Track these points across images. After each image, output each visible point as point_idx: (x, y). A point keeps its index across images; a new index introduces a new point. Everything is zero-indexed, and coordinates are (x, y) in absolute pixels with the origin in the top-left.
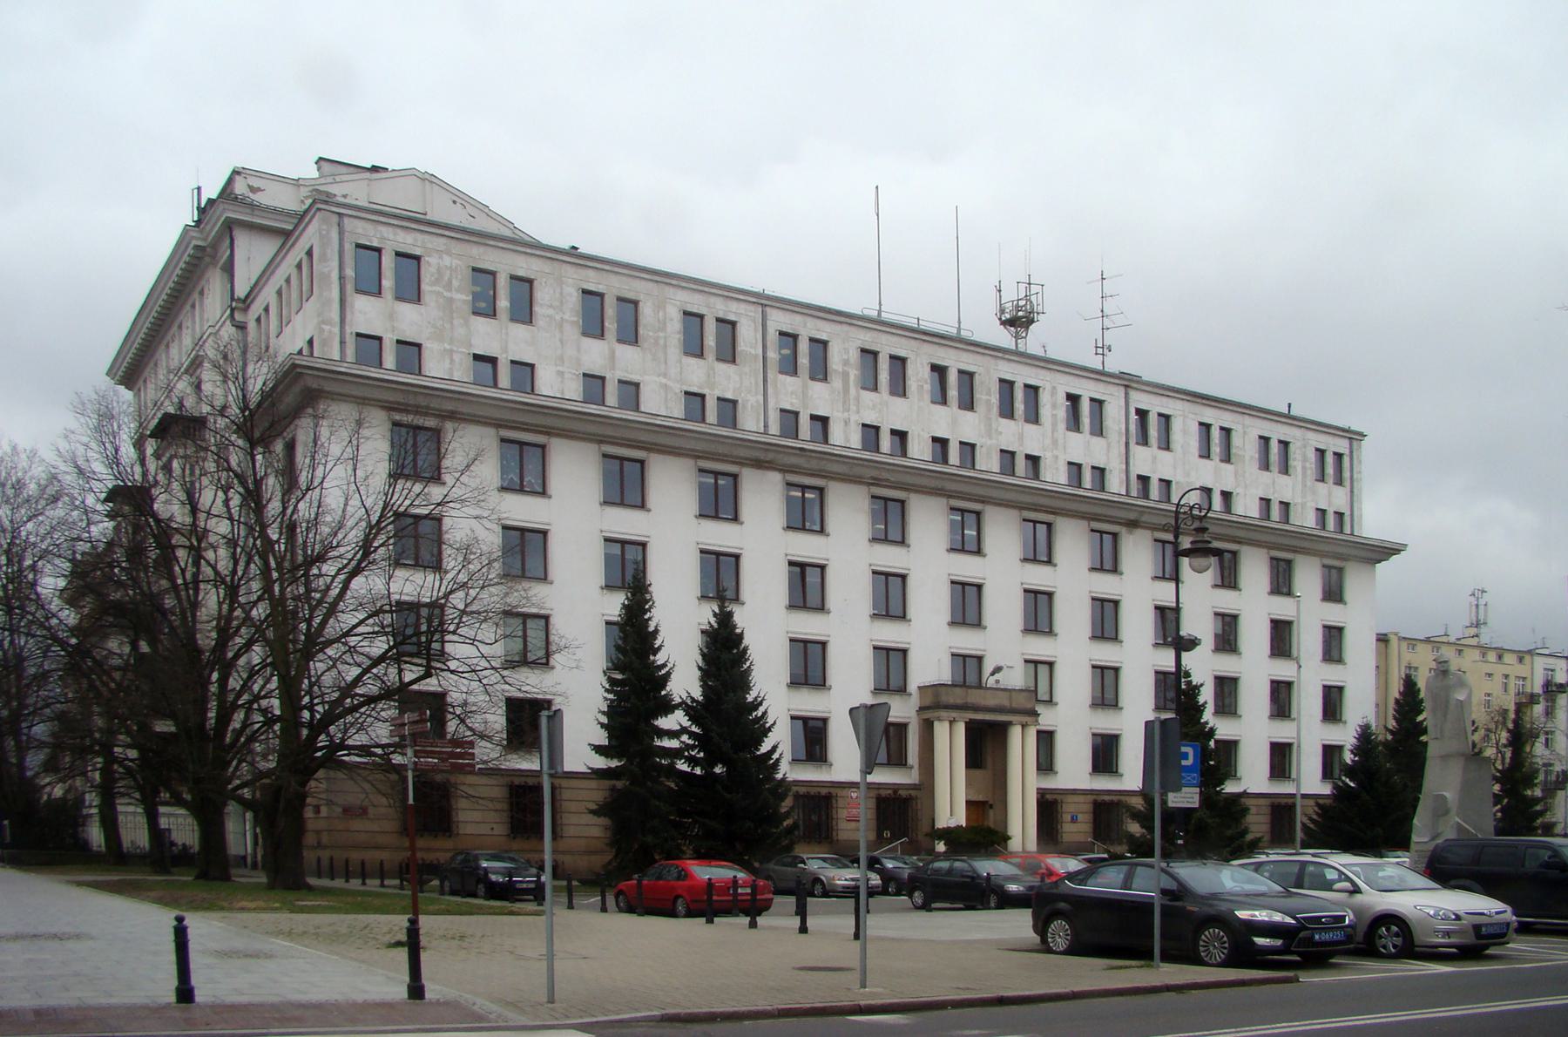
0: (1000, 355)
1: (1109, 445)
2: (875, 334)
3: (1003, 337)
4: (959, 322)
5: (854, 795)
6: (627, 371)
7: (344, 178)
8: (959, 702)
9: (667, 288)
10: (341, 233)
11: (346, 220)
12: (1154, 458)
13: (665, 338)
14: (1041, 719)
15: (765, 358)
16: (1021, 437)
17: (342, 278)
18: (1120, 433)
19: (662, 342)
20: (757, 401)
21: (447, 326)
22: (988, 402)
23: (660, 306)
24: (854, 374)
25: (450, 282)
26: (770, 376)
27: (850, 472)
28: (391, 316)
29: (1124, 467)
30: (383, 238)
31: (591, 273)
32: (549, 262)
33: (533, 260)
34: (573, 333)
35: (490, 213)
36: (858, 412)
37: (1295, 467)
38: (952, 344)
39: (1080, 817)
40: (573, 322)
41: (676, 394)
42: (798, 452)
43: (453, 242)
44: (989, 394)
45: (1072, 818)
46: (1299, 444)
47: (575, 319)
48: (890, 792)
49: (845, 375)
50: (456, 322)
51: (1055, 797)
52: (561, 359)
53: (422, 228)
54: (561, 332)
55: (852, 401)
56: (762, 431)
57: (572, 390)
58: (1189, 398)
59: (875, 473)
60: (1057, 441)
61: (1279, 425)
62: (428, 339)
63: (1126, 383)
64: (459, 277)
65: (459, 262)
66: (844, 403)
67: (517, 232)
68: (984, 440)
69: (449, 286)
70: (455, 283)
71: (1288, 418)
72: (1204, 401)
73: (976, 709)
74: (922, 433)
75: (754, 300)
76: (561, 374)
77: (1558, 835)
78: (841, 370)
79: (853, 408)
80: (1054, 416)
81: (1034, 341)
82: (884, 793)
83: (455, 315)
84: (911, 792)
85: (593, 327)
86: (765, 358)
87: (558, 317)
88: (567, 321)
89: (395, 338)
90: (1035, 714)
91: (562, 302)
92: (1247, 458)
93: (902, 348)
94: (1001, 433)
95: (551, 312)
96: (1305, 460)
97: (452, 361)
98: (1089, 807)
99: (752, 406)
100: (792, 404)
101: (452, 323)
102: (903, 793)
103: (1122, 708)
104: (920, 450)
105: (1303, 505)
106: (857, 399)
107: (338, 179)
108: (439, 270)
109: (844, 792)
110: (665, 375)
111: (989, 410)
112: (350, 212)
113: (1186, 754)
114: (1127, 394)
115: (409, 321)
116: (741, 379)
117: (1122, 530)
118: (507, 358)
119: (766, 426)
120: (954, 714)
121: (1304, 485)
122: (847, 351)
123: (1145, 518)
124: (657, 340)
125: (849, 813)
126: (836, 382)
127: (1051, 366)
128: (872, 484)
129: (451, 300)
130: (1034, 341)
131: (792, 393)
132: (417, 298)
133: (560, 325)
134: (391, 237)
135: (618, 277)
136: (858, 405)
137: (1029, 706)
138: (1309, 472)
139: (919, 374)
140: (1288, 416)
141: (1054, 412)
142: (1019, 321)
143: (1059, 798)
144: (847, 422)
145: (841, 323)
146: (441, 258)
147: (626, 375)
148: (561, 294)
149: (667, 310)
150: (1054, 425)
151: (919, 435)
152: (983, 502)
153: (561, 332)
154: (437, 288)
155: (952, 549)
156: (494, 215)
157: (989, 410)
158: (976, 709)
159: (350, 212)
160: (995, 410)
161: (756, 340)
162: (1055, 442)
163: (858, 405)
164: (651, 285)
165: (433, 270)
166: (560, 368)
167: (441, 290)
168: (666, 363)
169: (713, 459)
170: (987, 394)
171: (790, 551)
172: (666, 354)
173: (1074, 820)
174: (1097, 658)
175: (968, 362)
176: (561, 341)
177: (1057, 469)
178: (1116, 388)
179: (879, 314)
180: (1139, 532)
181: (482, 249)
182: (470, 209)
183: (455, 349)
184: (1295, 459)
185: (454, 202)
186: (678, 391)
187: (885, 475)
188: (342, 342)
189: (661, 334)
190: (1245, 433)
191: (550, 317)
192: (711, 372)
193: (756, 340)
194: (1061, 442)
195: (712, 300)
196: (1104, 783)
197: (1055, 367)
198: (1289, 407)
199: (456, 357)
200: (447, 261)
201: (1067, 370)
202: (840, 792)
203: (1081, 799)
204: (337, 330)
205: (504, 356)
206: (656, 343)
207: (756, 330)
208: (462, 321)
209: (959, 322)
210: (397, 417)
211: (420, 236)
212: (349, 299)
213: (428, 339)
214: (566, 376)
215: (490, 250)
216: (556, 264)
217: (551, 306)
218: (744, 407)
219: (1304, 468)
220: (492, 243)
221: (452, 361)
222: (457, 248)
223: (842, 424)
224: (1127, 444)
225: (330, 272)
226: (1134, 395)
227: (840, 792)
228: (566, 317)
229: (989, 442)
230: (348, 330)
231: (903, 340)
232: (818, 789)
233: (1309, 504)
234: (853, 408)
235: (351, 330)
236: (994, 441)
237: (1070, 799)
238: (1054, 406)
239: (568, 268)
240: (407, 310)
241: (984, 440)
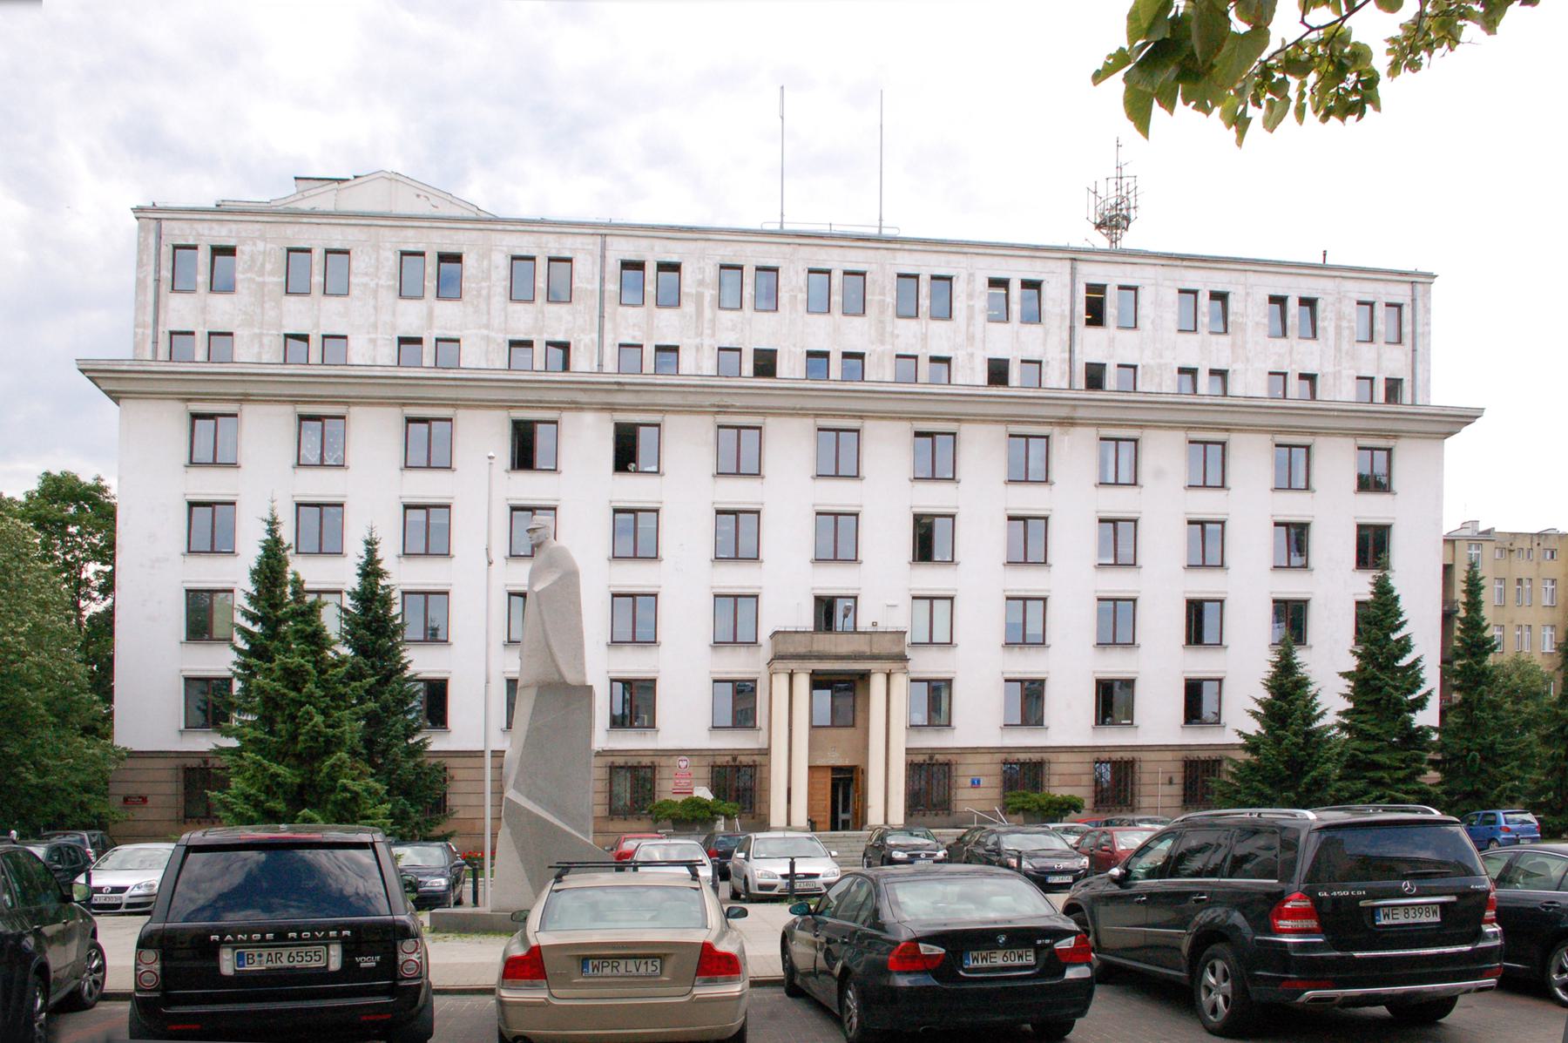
0: (898, 246)
1: (1046, 333)
2: (737, 246)
3: (1101, 241)
4: (881, 220)
5: (683, 764)
6: (446, 329)
7: (312, 192)
8: (802, 650)
9: (494, 235)
10: (159, 237)
11: (164, 224)
12: (542, 312)
13: (489, 287)
14: (910, 665)
15: (602, 292)
16: (925, 338)
17: (158, 281)
18: (1062, 316)
19: (484, 292)
20: (592, 340)
21: (258, 311)
22: (882, 303)
23: (485, 255)
24: (710, 294)
25: (263, 265)
26: (608, 310)
27: (887, 407)
28: (204, 309)
29: (1067, 355)
30: (199, 235)
31: (410, 233)
32: (366, 229)
33: (350, 230)
34: (388, 297)
35: (454, 201)
36: (713, 335)
37: (1325, 329)
38: (834, 243)
39: (968, 782)
40: (389, 286)
41: (499, 344)
42: (616, 387)
43: (268, 226)
44: (883, 293)
45: (973, 783)
46: (1330, 299)
47: (392, 283)
48: (729, 758)
49: (699, 297)
50: (267, 306)
51: (949, 757)
52: (375, 326)
53: (235, 218)
54: (376, 298)
55: (706, 325)
56: (596, 370)
57: (386, 354)
58: (1163, 262)
59: (716, 400)
60: (973, 337)
61: (1301, 279)
62: (238, 326)
63: (1073, 256)
64: (273, 260)
65: (274, 246)
66: (697, 327)
67: (479, 212)
68: (874, 347)
69: (261, 273)
70: (268, 267)
71: (1322, 269)
72: (1185, 263)
73: (821, 657)
74: (793, 349)
75: (591, 231)
76: (373, 341)
77: (777, 829)
78: (694, 291)
79: (707, 331)
80: (971, 308)
81: (1129, 240)
82: (720, 760)
83: (266, 298)
84: (756, 758)
85: (518, 293)
86: (602, 292)
87: (372, 284)
88: (382, 286)
89: (207, 331)
90: (902, 658)
91: (377, 268)
92: (1250, 324)
93: (856, 259)
94: (898, 336)
95: (365, 280)
96: (1340, 317)
97: (261, 345)
98: (997, 769)
99: (585, 346)
100: (634, 337)
101: (263, 307)
102: (745, 760)
103: (1226, 647)
104: (880, 371)
105: (1337, 375)
106: (713, 321)
107: (306, 194)
108: (253, 259)
109: (671, 761)
110: (487, 326)
111: (882, 312)
112: (165, 216)
113: (308, 713)
114: (1073, 269)
115: (222, 311)
116: (574, 318)
117: (1055, 432)
118: (317, 334)
119: (600, 365)
120: (793, 665)
121: (1338, 349)
122: (702, 270)
123: (1080, 413)
124: (479, 291)
125: (676, 784)
126: (688, 306)
127: (966, 250)
128: (718, 413)
129: (263, 284)
130: (1129, 240)
131: (634, 325)
132: (230, 289)
133: (375, 292)
134: (206, 232)
135: (440, 232)
136: (713, 328)
137: (896, 650)
138: (1346, 333)
139: (793, 281)
140: (1323, 267)
141: (971, 303)
142: (1113, 222)
143: (952, 758)
144: (699, 348)
145: (696, 240)
146: (255, 244)
147: (446, 332)
148: (377, 259)
149: (493, 257)
150: (970, 318)
151: (790, 351)
152: (861, 417)
153: (376, 298)
154: (249, 275)
155: (818, 476)
156: (458, 202)
157: (882, 312)
158: (821, 657)
159: (165, 216)
160: (891, 311)
161: (593, 274)
162: (971, 338)
163: (713, 328)
164: (474, 233)
165: (246, 257)
166: (373, 336)
167: (253, 276)
168: (489, 314)
169: (834, 416)
170: (880, 294)
171: (717, 499)
172: (488, 305)
173: (975, 784)
174: (1012, 587)
175: (856, 259)
176: (375, 308)
177: (972, 369)
178: (1059, 263)
179: (782, 227)
180: (1079, 430)
181: (297, 228)
182: (434, 200)
183: (265, 332)
184: (1324, 319)
185: (418, 196)
186: (500, 341)
187: (728, 401)
188: (155, 342)
189: (484, 284)
190: (1247, 294)
191: (365, 285)
192: (540, 316)
193: (593, 274)
194: (979, 336)
195: (545, 238)
196: (1113, 737)
197: (972, 250)
198: (1325, 255)
199: (266, 340)
200: (261, 246)
201: (947, 249)
202: (663, 761)
203: (986, 758)
204: (150, 332)
205: (315, 331)
206: (479, 295)
207: (594, 263)
208: (273, 304)
209: (881, 220)
210: (724, 419)
211: (234, 226)
212: (162, 298)
213: (238, 326)
214: (380, 342)
215: (305, 227)
216: (372, 230)
217: (366, 274)
218: (576, 348)
219: (1338, 329)
220: (305, 220)
221: (261, 345)
222: (271, 231)
223: (694, 350)
224: (1072, 328)
225: (145, 277)
226: (1081, 267)
227: (663, 761)
228: (382, 282)
229: (880, 348)
230: (161, 329)
231: (774, 247)
232: (640, 759)
233: (1345, 373)
234: (707, 331)
235: (164, 330)
236: (888, 347)
237: (970, 759)
238: (970, 296)
239: (386, 231)
240: (220, 302)
241: (874, 347)
